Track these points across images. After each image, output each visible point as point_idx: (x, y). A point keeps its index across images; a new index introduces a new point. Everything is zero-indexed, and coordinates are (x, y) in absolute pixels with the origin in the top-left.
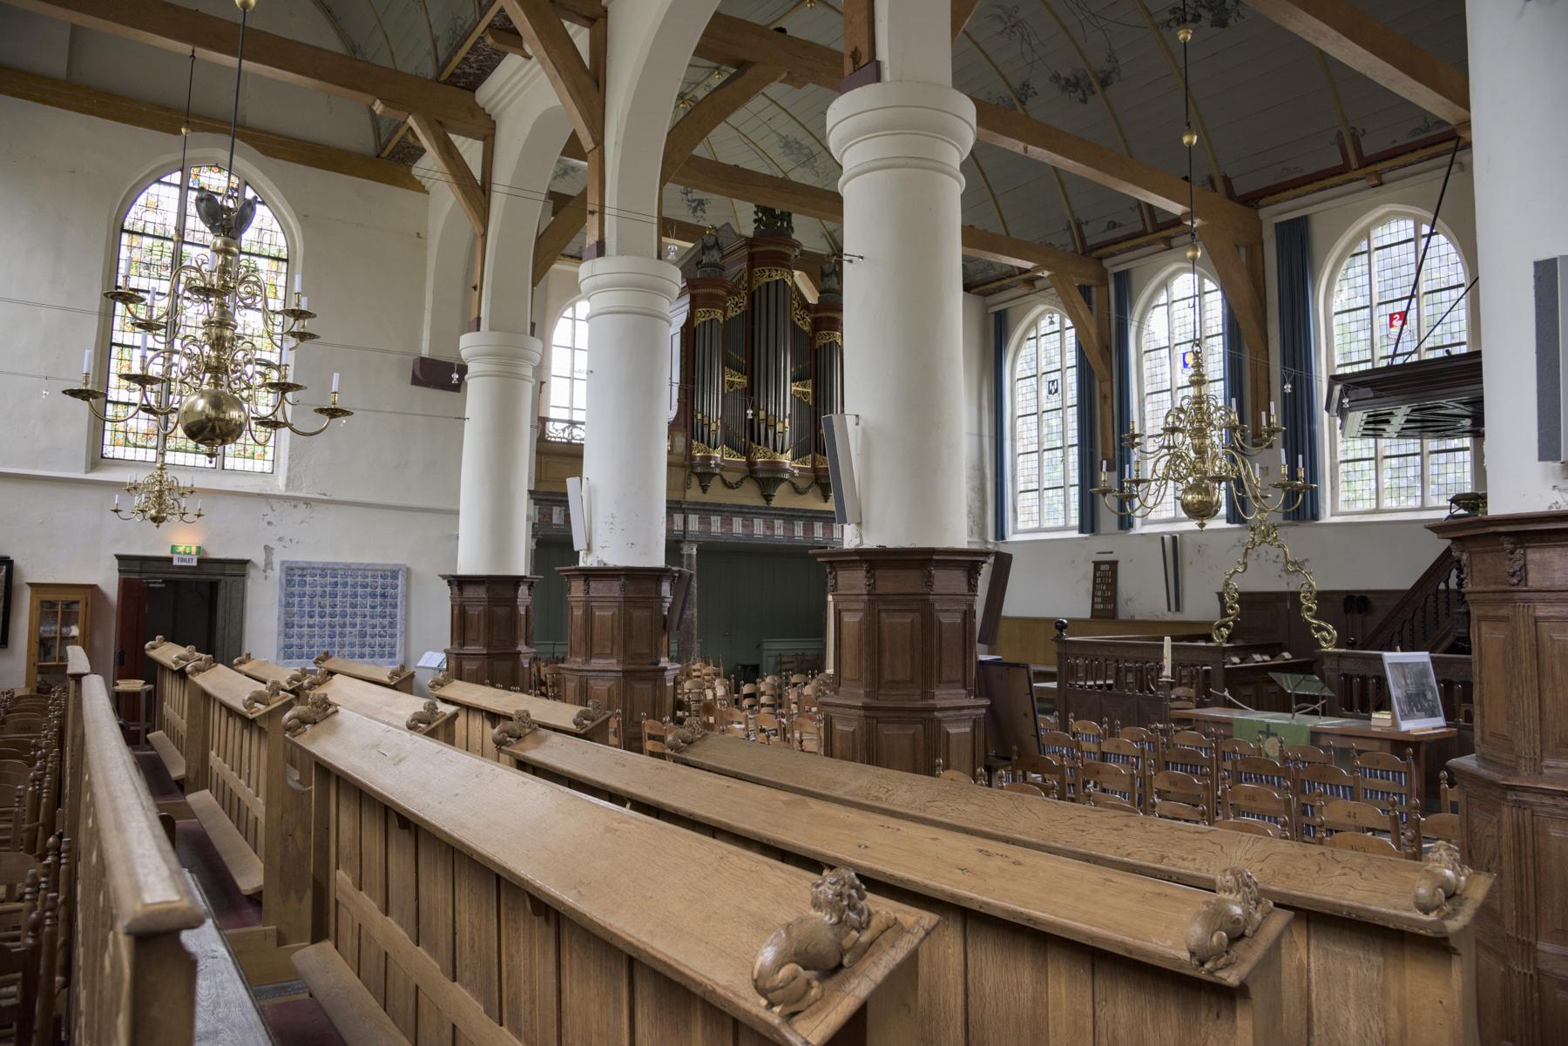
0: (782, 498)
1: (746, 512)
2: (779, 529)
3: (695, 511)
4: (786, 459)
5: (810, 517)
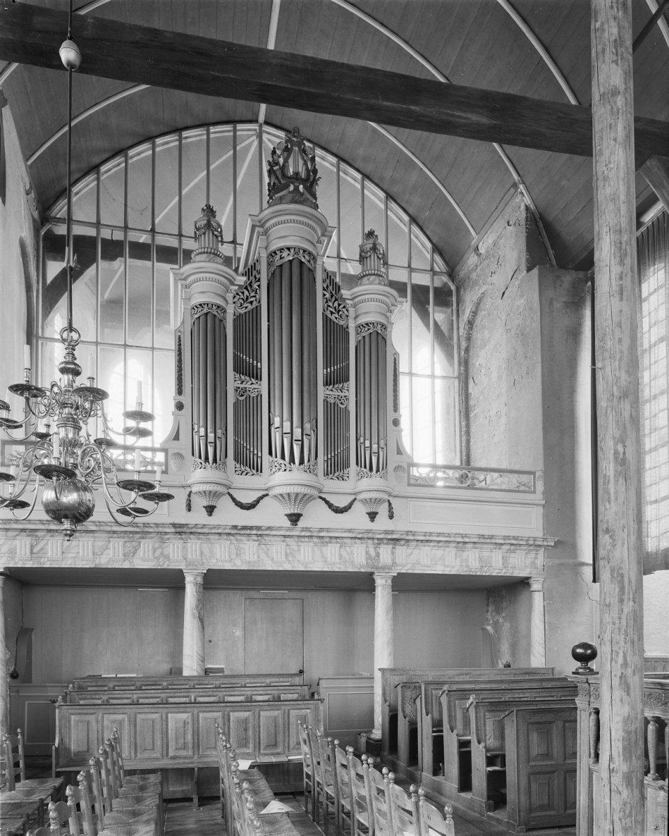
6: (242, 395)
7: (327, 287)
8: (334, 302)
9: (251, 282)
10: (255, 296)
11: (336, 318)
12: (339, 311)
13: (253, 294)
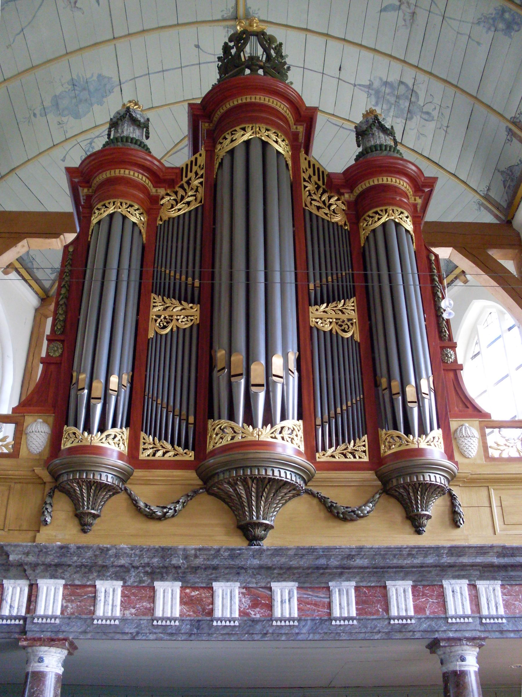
0: (290, 527)
1: (198, 573)
2: (286, 599)
3: (53, 570)
4: (287, 441)
5: (374, 572)
6: (165, 327)
7: (310, 177)
8: (322, 195)
9: (190, 179)
10: (195, 195)
11: (326, 214)
12: (331, 205)
13: (190, 193)
